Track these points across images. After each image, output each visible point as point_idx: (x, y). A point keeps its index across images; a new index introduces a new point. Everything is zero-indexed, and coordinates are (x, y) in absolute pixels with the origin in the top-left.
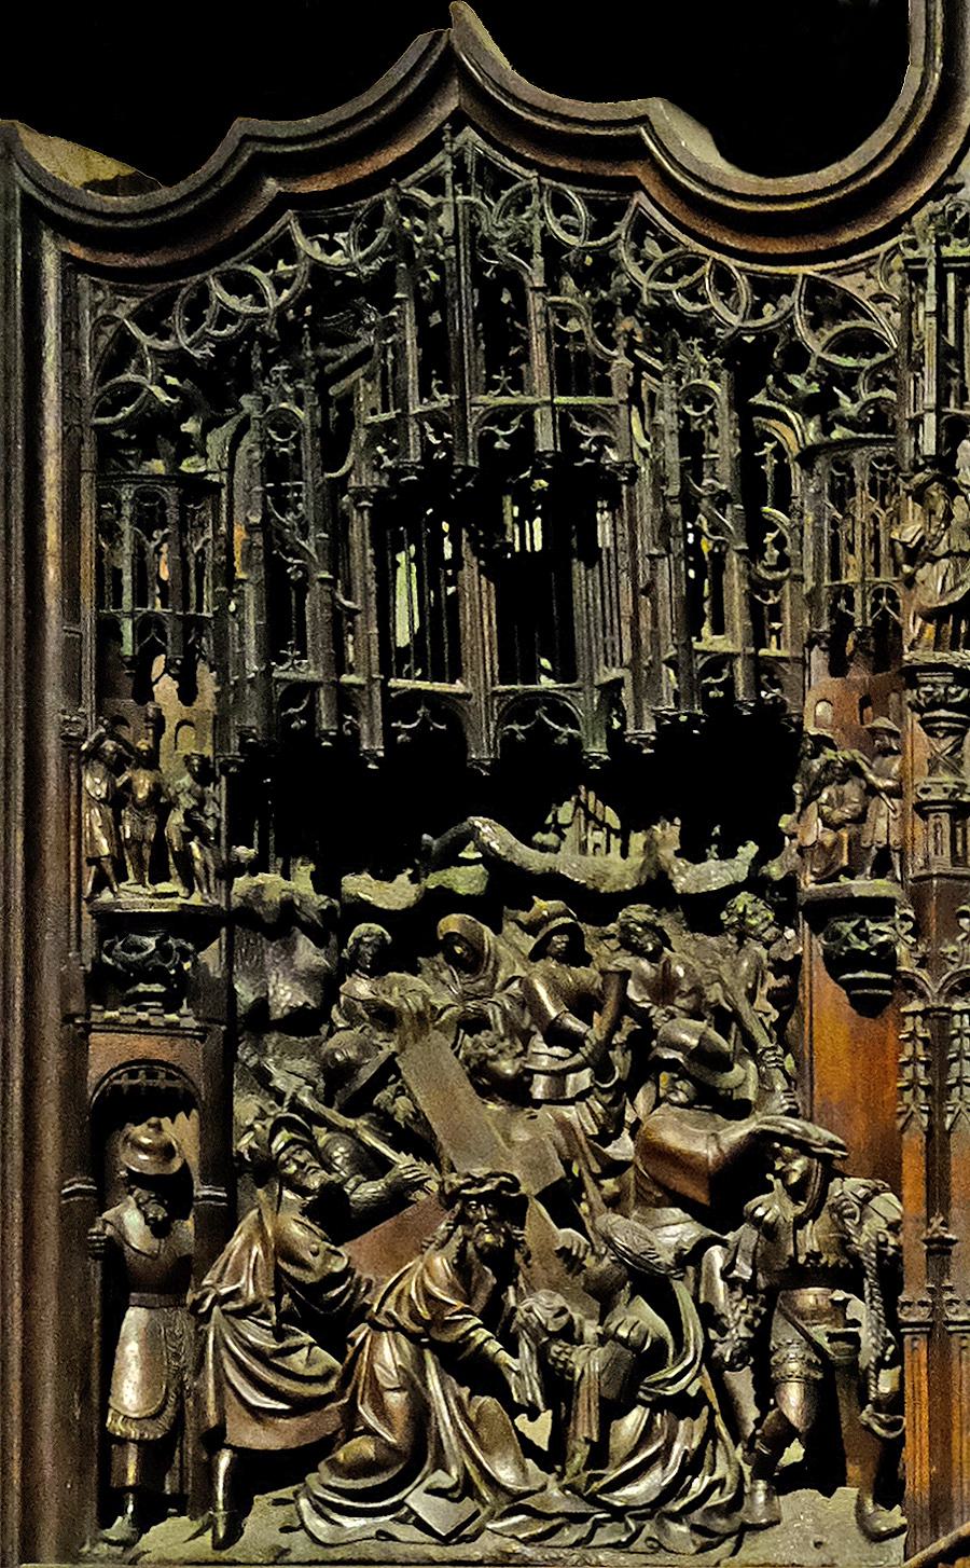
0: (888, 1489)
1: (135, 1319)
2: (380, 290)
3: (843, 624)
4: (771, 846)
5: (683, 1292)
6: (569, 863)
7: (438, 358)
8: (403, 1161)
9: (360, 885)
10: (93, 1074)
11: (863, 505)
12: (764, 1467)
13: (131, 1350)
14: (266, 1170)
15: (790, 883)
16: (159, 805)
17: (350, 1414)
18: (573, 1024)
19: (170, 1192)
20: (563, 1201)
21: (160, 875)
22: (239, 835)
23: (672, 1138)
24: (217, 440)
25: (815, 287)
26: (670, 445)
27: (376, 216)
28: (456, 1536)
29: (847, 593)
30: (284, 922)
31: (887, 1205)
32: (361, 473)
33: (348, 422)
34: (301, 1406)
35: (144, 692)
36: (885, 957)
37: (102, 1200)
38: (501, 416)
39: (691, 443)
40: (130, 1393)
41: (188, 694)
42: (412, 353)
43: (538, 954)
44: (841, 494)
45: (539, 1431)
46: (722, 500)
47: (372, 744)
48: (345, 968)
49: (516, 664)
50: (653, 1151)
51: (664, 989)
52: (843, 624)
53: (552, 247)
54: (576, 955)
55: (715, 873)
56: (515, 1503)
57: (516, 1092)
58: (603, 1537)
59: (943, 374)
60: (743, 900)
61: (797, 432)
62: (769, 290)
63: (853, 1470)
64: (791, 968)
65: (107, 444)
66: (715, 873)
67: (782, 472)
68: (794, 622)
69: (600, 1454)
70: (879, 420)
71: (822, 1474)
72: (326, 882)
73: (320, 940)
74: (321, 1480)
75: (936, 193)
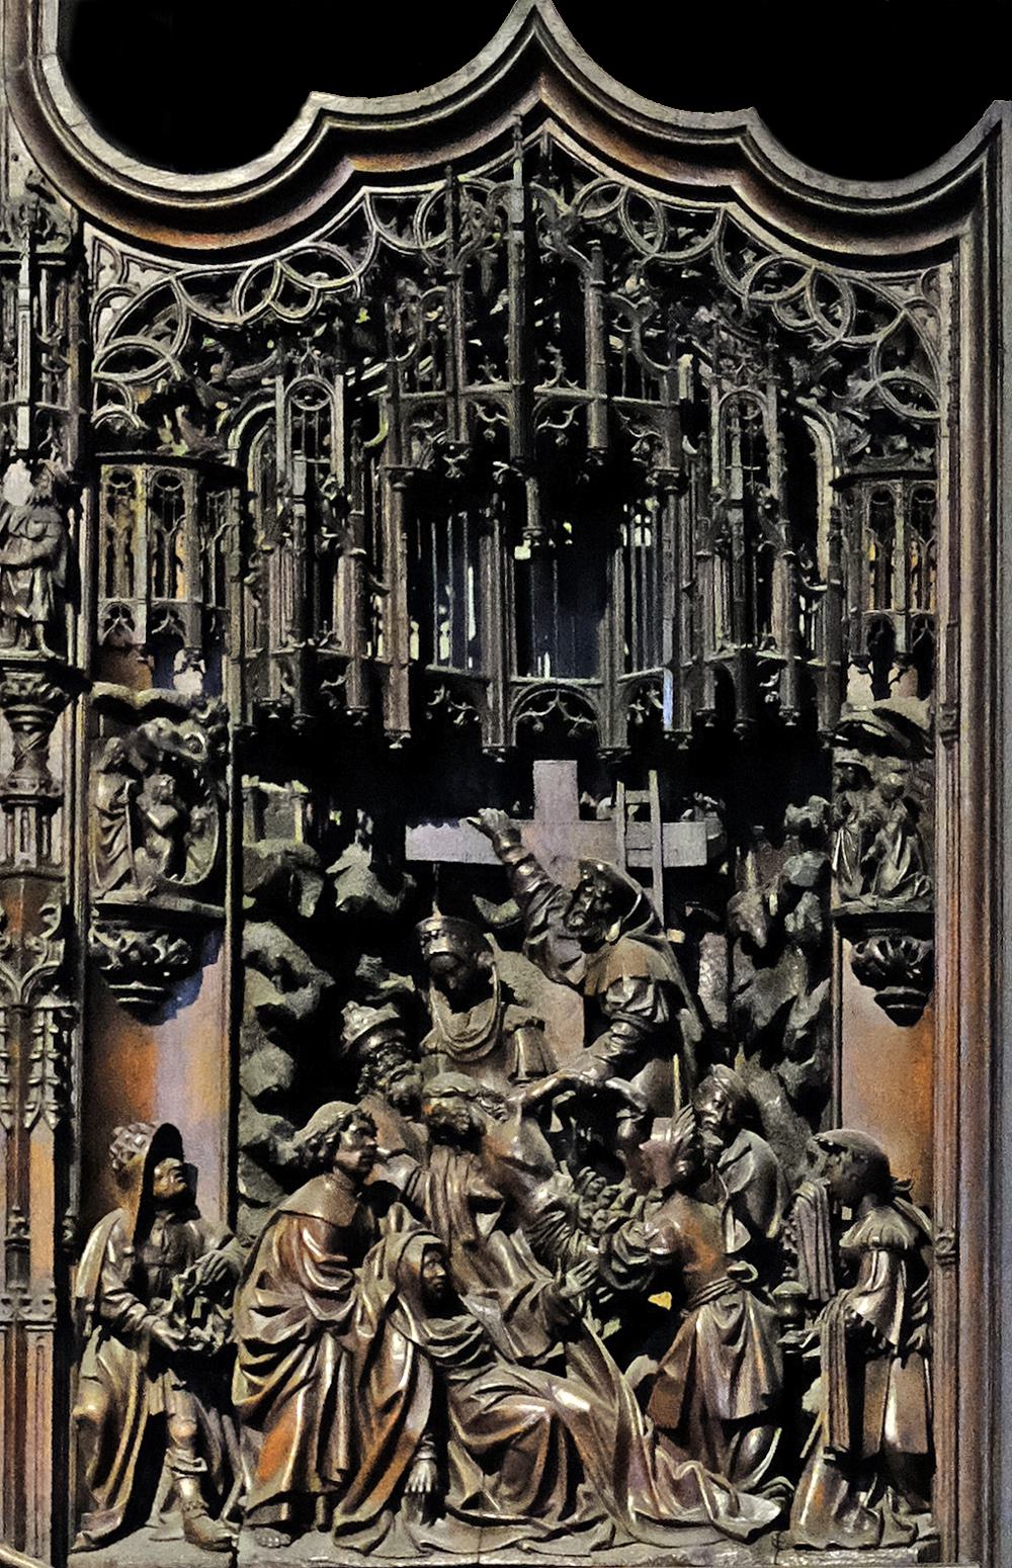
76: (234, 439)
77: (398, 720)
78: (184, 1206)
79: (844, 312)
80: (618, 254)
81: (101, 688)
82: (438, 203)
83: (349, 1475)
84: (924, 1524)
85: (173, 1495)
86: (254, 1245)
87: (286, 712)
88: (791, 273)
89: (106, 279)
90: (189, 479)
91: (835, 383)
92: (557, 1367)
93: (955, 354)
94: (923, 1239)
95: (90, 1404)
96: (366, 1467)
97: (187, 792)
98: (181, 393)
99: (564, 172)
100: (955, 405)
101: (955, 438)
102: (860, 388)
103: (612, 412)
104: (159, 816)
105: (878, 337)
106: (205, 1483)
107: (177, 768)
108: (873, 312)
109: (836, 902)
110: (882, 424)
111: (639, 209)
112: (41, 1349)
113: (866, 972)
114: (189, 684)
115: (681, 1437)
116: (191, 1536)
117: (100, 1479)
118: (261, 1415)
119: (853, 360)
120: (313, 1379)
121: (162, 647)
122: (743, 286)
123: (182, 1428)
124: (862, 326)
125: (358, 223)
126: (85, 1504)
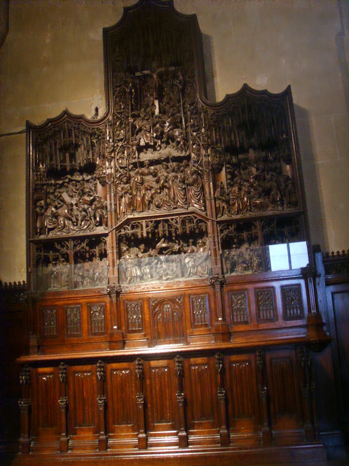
0: (107, 225)
3: (100, 155)
5: (87, 211)
6: (76, 179)
16: (40, 175)
17: (58, 223)
18: (76, 191)
25: (97, 128)
29: (101, 152)
36: (105, 182)
41: (43, 166)
43: (73, 186)
46: (89, 146)
47: (59, 168)
49: (71, 161)
50: (84, 200)
53: (74, 127)
58: (81, 232)
60: (91, 180)
63: (103, 225)
64: (96, 184)
67: (94, 144)
69: (81, 225)
74: (56, 230)
75: (107, 120)
76: (221, 125)
81: (212, 146)
83: (242, 209)
85: (225, 212)
90: (218, 128)
96: (243, 208)
109: (281, 155)
112: (213, 201)
114: (219, 145)
118: (234, 204)
123: (226, 207)
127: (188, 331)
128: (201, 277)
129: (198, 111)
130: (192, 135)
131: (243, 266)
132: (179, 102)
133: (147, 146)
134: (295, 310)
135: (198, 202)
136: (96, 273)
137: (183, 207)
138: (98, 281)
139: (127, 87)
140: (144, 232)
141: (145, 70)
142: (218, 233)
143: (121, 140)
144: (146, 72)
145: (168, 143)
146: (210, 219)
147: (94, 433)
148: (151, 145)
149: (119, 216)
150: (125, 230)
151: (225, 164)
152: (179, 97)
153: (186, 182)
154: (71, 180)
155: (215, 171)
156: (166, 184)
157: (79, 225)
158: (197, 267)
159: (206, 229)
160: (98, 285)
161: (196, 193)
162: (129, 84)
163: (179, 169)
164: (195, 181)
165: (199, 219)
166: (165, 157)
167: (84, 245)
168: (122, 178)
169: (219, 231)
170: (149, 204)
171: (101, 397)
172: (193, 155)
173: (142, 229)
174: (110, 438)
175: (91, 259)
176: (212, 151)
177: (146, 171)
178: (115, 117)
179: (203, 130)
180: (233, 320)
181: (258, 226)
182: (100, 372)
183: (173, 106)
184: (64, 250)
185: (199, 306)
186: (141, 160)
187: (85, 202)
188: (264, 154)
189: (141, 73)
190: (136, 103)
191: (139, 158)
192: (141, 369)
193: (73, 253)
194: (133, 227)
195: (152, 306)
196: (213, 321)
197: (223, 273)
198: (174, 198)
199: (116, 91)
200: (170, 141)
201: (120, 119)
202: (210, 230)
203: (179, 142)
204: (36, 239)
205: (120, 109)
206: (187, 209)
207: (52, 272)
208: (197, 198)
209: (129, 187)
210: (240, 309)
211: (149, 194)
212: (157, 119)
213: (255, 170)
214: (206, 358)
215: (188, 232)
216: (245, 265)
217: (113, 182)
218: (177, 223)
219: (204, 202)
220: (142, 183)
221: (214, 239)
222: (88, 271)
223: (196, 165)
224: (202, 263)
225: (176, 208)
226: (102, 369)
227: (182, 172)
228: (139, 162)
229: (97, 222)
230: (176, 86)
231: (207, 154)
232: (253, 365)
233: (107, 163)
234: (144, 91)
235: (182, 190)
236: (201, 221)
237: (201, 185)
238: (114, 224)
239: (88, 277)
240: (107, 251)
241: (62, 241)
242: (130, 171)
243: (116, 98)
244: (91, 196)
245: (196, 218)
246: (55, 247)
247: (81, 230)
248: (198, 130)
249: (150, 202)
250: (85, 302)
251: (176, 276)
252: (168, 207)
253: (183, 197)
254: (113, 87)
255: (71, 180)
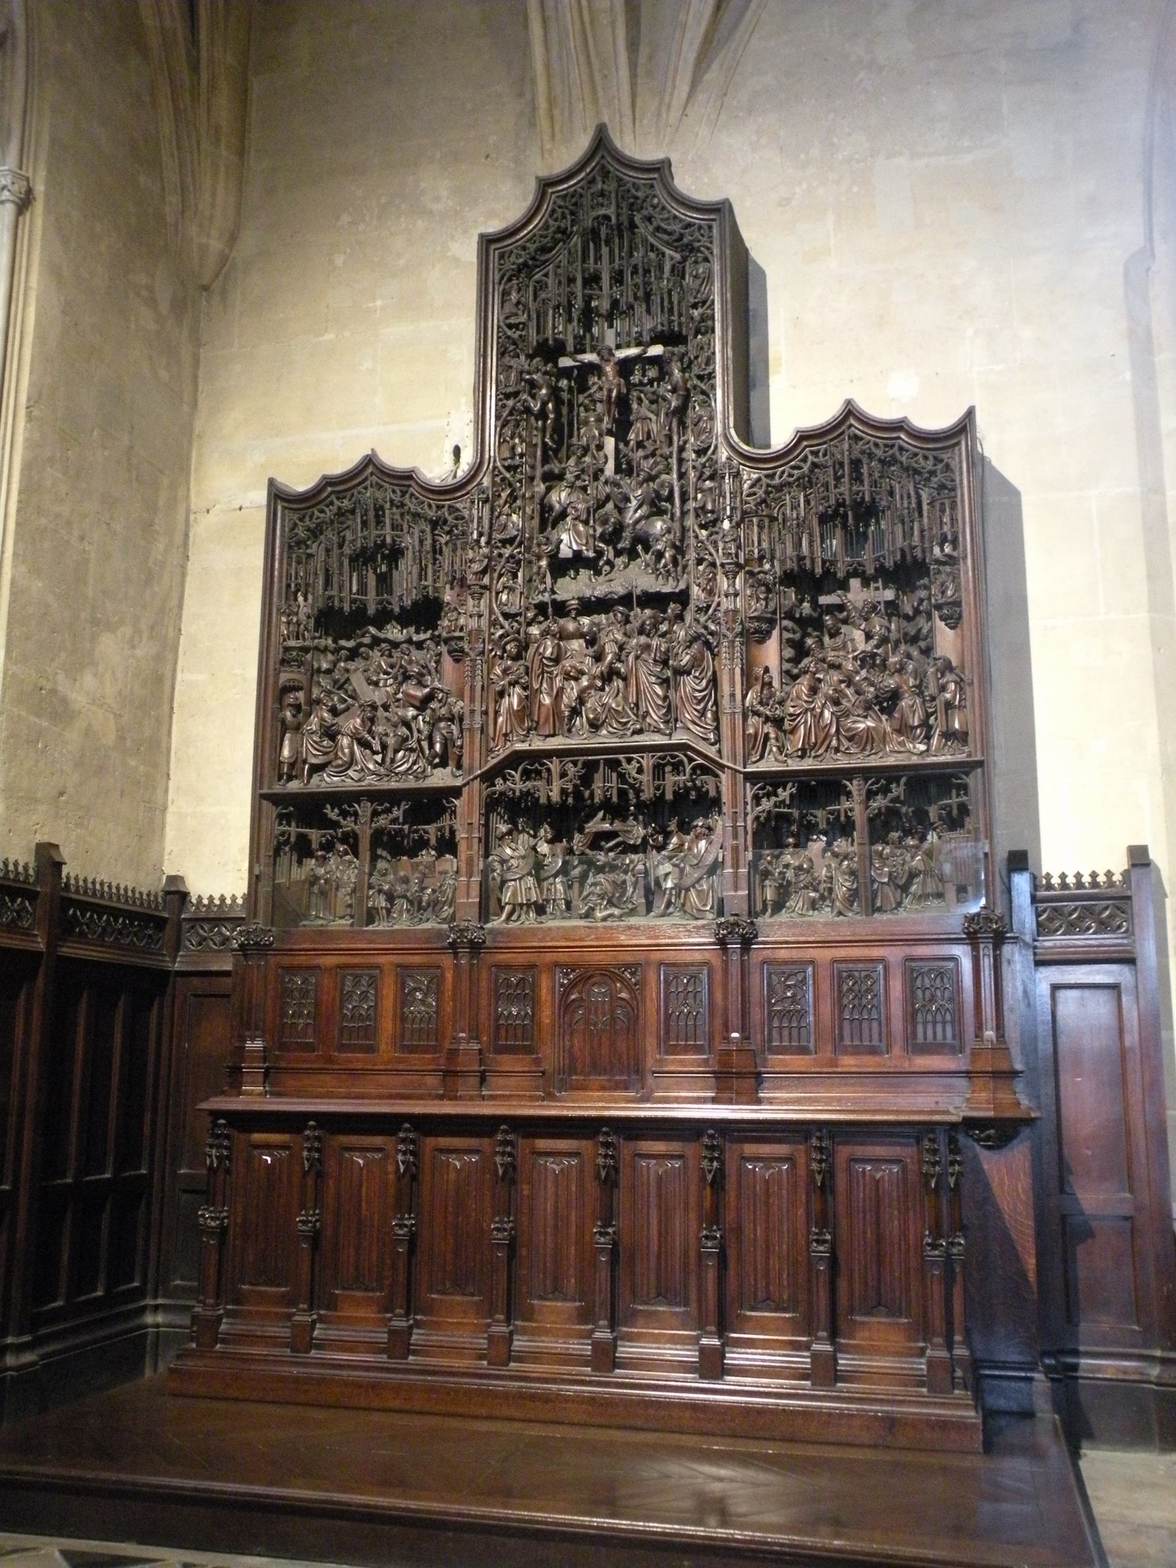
0: (459, 766)
1: (288, 735)
2: (353, 512)
3: (454, 578)
4: (435, 628)
5: (413, 725)
6: (390, 636)
7: (365, 524)
8: (350, 700)
9: (343, 643)
10: (281, 681)
11: (459, 552)
12: (430, 763)
13: (286, 743)
14: (318, 702)
15: (439, 636)
16: (298, 624)
17: (336, 754)
19: (297, 708)
20: (386, 707)
21: (298, 638)
22: (316, 631)
23: (412, 692)
24: (315, 546)
25: (450, 507)
26: (417, 543)
27: (352, 495)
28: (360, 780)
30: (325, 650)
31: (461, 703)
32: (347, 550)
33: (344, 540)
34: (325, 754)
35: (296, 599)
36: (462, 650)
37: (281, 709)
38: (379, 536)
39: (421, 542)
40: (286, 752)
41: (306, 600)
42: (359, 526)
44: (454, 550)
45: (379, 758)
46: (428, 552)
47: (347, 608)
48: (339, 660)
50: (406, 694)
51: (410, 662)
52: (454, 578)
53: (392, 501)
54: (390, 656)
55: (422, 636)
56: (373, 773)
57: (376, 684)
59: (478, 522)
60: (428, 642)
61: (444, 539)
62: (439, 507)
63: (450, 762)
64: (440, 654)
65: (290, 547)
66: (422, 636)
67: (441, 548)
68: (443, 578)
69: (393, 761)
70: (464, 533)
71: (444, 764)
72: (335, 642)
73: (333, 653)
74: (329, 770)
77: (819, 570)
78: (770, 684)
79: (931, 462)
80: (871, 456)
82: (826, 450)
83: (815, 744)
84: (966, 749)
85: (771, 750)
86: (788, 694)
87: (792, 570)
88: (916, 455)
89: (745, 477)
90: (767, 520)
91: (928, 479)
92: (866, 717)
93: (961, 468)
94: (962, 680)
95: (751, 731)
97: (769, 591)
98: (764, 501)
99: (857, 438)
100: (961, 480)
101: (962, 488)
102: (934, 480)
103: (871, 492)
104: (762, 596)
105: (940, 466)
106: (779, 748)
107: (766, 585)
108: (938, 460)
109: (933, 601)
110: (942, 487)
111: (876, 445)
112: (739, 719)
113: (941, 618)
115: (899, 731)
116: (776, 760)
117: (753, 748)
118: (793, 731)
119: (932, 473)
120: (806, 722)
121: (761, 558)
122: (904, 459)
123: (772, 735)
124: (935, 465)
125: (806, 457)
126: (750, 754)
127: (650, 1064)
128: (697, 919)
129: (716, 470)
130: (696, 537)
131: (809, 897)
132: (671, 444)
133: (578, 561)
134: (939, 1028)
135: (700, 718)
136: (426, 888)
137: (658, 731)
138: (430, 909)
139: (533, 397)
140: (552, 791)
141: (584, 352)
142: (746, 803)
143: (510, 541)
144: (590, 357)
145: (633, 555)
146: (729, 768)
147: (379, 1312)
148: (588, 559)
149: (492, 744)
150: (505, 780)
151: (781, 619)
152: (670, 429)
153: (671, 662)
154: (377, 641)
155: (754, 635)
156: (619, 665)
157: (388, 760)
158: (688, 890)
159: (719, 792)
160: (428, 920)
161: (697, 694)
162: (540, 388)
163: (655, 626)
164: (697, 662)
165: (701, 766)
166: (621, 591)
167: (397, 813)
168: (506, 644)
169: (749, 799)
170: (571, 718)
171: (402, 1219)
172: (695, 591)
173: (549, 782)
174: (418, 1328)
175: (413, 853)
176: (746, 581)
177: (571, 626)
178: (498, 479)
179: (726, 525)
180: (770, 1040)
181: (855, 793)
182: (404, 1153)
183: (653, 454)
184: (348, 824)
185: (682, 995)
186: (559, 598)
187: (409, 701)
188: (889, 594)
189: (575, 360)
190: (559, 443)
191: (553, 592)
192: (510, 1154)
193: (369, 832)
194: (527, 775)
195: (562, 985)
196: (718, 1039)
197: (751, 913)
198: (637, 705)
199: (504, 406)
200: (639, 548)
201: (510, 485)
202: (726, 797)
203: (660, 555)
204: (278, 788)
205: (512, 458)
206: (670, 735)
207: (314, 880)
208: (698, 708)
209: (522, 669)
210: (789, 1011)
211: (572, 689)
212: (608, 489)
213: (863, 637)
214: (680, 1144)
215: (669, 796)
216: (812, 894)
217: (482, 653)
218: (640, 771)
219: (716, 719)
220: (557, 660)
221: (735, 820)
222: (406, 881)
223: (703, 619)
224: (699, 880)
225: (639, 732)
226: (412, 1147)
227: (663, 635)
228: (554, 602)
229: (436, 755)
230: (665, 399)
231: (731, 591)
232: (802, 1171)
233: (470, 602)
234: (582, 409)
235: (660, 684)
236: (705, 770)
237: (710, 673)
238: (477, 764)
239: (404, 897)
240: (457, 833)
241: (344, 800)
242: (529, 624)
243: (503, 426)
244: (426, 687)
245: (691, 760)
246: (326, 814)
247: (391, 773)
248: (714, 523)
249: (575, 712)
250: (391, 963)
251: (632, 910)
252: (619, 727)
253: (660, 702)
254: (497, 395)
255: (377, 641)
